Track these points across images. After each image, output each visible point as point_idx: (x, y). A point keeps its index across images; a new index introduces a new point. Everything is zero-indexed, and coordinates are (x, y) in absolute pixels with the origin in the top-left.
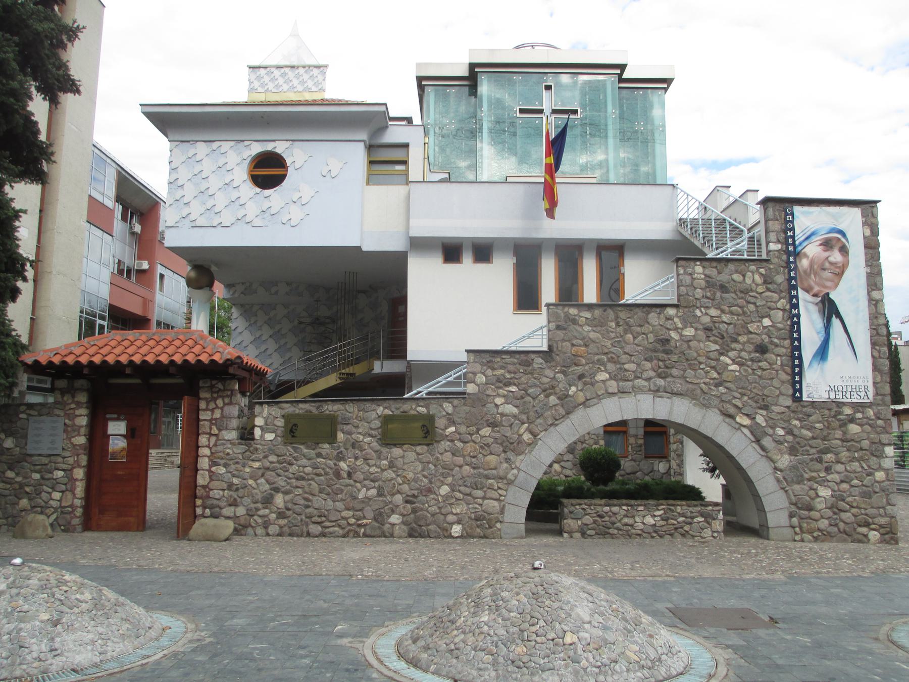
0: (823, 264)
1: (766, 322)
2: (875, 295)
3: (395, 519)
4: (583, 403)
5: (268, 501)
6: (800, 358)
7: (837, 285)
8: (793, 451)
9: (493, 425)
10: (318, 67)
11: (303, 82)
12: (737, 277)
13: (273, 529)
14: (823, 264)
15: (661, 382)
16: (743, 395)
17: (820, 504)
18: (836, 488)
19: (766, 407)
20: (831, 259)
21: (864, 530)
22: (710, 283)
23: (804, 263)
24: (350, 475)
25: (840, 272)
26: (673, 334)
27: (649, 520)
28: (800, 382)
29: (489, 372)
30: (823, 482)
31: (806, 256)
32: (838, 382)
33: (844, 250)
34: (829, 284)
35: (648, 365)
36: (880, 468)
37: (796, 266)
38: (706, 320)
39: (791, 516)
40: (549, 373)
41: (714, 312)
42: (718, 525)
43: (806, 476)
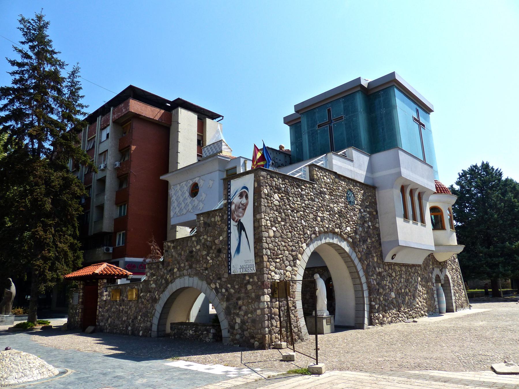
0: (239, 206)
1: (221, 238)
2: (258, 217)
3: (130, 328)
4: (171, 281)
5: (107, 320)
6: (230, 254)
7: (243, 215)
8: (228, 300)
9: (150, 292)
10: (220, 141)
11: (216, 149)
12: (213, 219)
13: (108, 330)
14: (239, 206)
15: (190, 271)
16: (213, 274)
17: (237, 327)
18: (242, 318)
19: (220, 279)
20: (242, 202)
21: (252, 341)
22: (205, 223)
23: (233, 207)
24: (122, 311)
25: (244, 207)
26: (194, 249)
27: (191, 332)
28: (230, 265)
29: (150, 272)
30: (238, 315)
31: (234, 203)
32: (243, 264)
33: (247, 197)
34: (241, 215)
35: (187, 264)
36: (259, 308)
37: (231, 209)
38: (203, 241)
39: (229, 332)
40: (163, 270)
41: (205, 237)
42: (211, 336)
43: (232, 312)
